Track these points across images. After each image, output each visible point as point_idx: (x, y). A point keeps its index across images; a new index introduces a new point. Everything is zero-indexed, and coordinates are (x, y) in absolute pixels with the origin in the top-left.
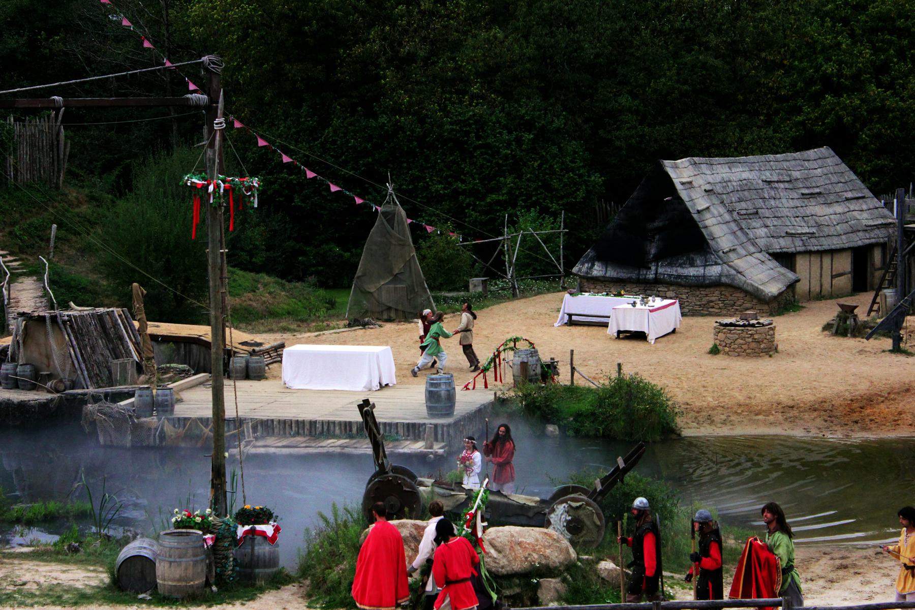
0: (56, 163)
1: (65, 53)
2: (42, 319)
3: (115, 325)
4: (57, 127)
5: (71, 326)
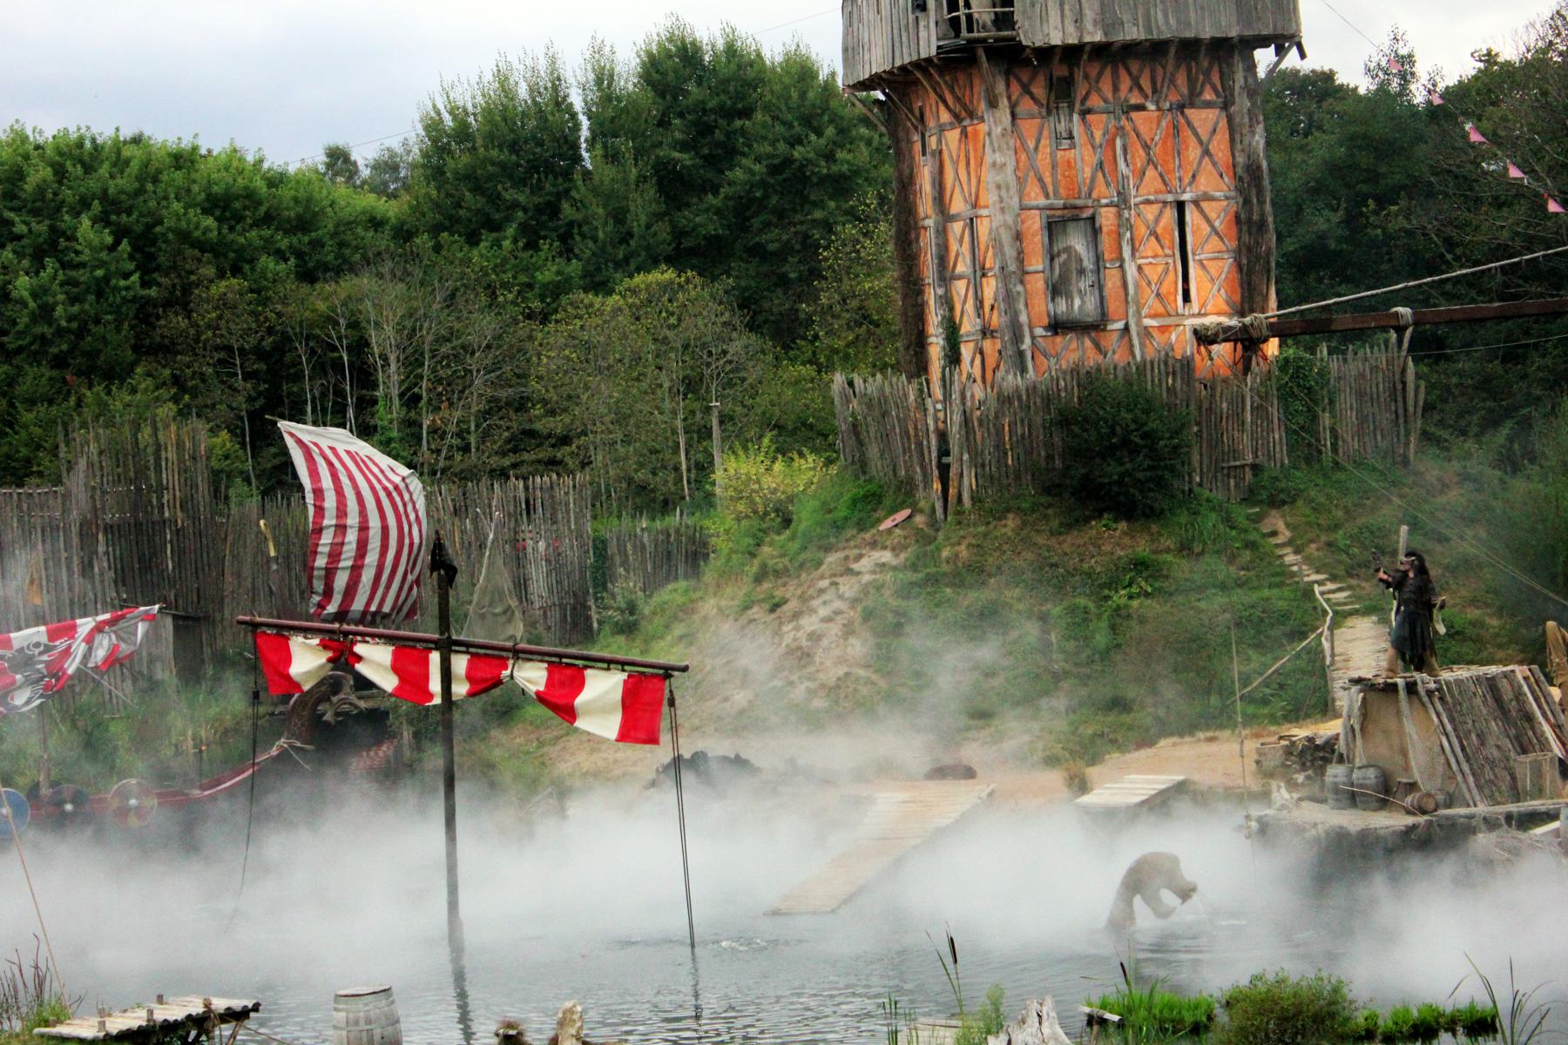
0: (1401, 420)
1: (1410, 233)
2: (1391, 689)
3: (1519, 695)
4: (1402, 360)
5: (1442, 699)
